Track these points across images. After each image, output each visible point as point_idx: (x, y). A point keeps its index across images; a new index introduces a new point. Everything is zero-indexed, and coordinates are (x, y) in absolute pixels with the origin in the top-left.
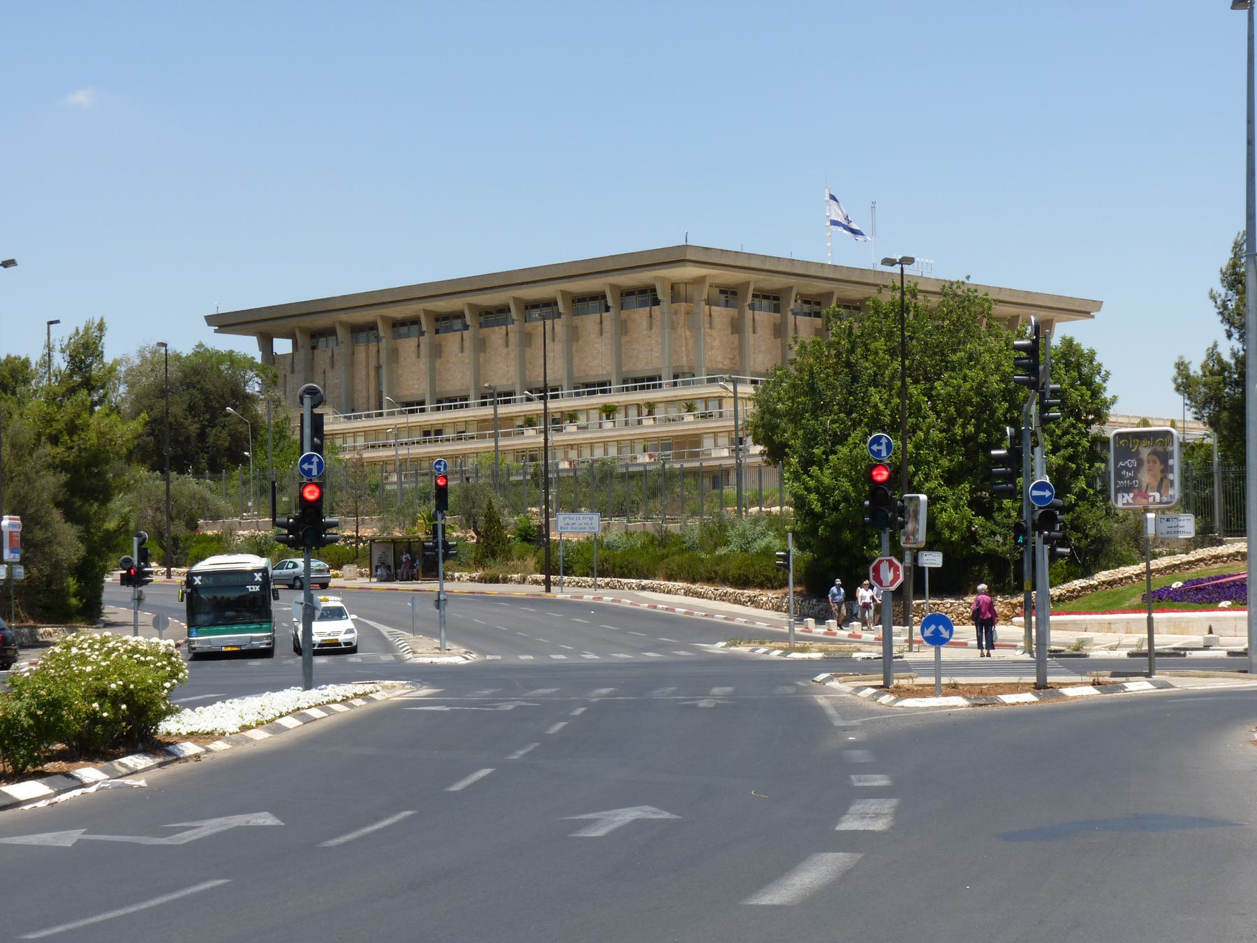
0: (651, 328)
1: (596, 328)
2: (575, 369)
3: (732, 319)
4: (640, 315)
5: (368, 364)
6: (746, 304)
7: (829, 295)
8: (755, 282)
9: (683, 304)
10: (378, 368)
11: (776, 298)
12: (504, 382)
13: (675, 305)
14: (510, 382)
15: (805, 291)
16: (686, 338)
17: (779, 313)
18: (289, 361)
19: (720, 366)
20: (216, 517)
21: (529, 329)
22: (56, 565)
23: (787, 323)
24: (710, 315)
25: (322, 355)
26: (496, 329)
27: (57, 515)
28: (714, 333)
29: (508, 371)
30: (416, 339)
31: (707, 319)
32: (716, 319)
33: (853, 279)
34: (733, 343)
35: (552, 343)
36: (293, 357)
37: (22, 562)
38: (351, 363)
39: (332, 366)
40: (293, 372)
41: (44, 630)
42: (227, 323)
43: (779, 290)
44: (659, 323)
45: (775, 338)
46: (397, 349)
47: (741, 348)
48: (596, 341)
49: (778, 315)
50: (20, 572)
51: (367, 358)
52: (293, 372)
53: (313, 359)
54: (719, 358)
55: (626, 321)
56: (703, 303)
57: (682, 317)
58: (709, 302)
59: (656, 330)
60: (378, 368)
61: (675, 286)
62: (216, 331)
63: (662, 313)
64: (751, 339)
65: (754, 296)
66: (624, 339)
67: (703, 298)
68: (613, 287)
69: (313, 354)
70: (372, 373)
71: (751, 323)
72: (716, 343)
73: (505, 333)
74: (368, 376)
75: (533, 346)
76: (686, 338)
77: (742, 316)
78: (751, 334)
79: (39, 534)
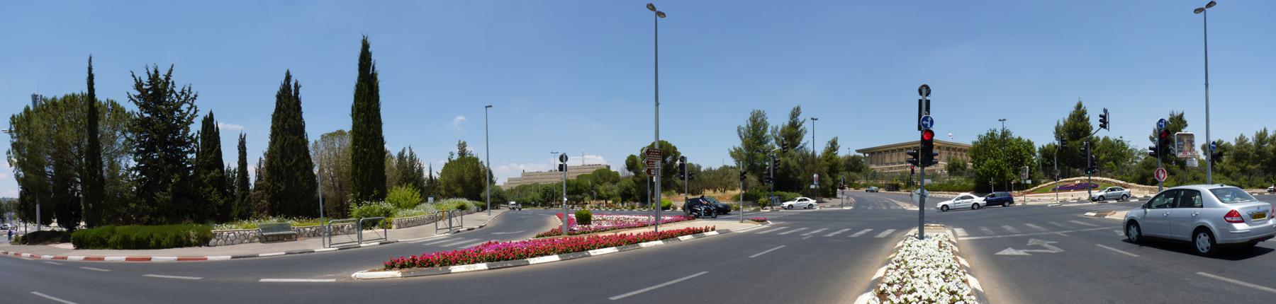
20: (857, 180)
22: (827, 186)
27: (827, 176)
37: (819, 185)
41: (824, 199)
50: (818, 187)
79: (823, 179)
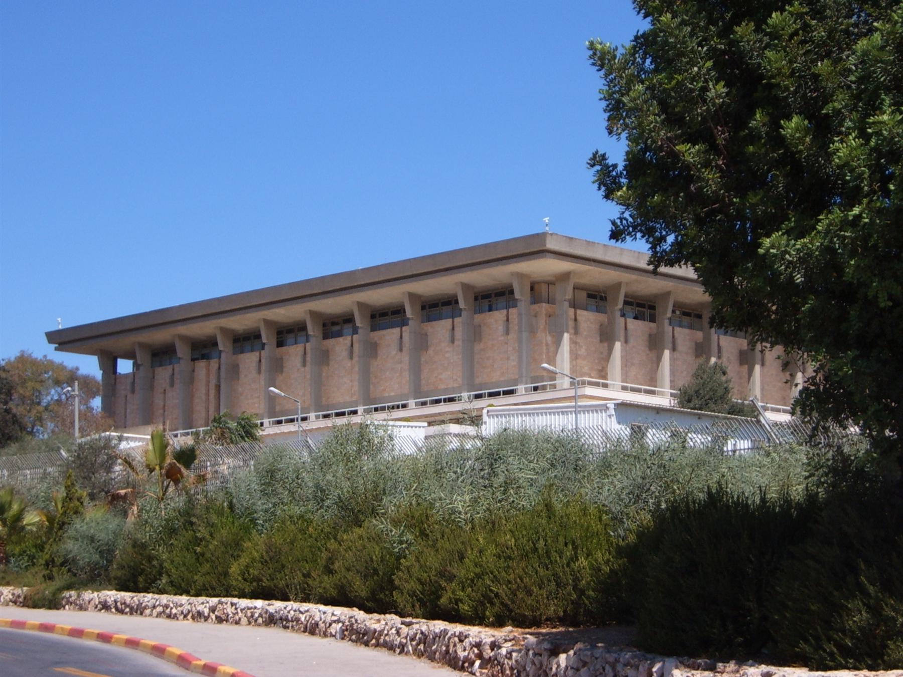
0: (507, 332)
1: (447, 335)
2: (423, 382)
4: (495, 319)
5: (208, 383)
10: (218, 387)
13: (536, 306)
16: (547, 345)
18: (130, 380)
21: (376, 339)
25: (163, 374)
29: (352, 386)
30: (258, 354)
35: (399, 353)
36: (134, 376)
38: (191, 380)
39: (172, 384)
40: (133, 391)
42: (67, 339)
44: (516, 328)
46: (238, 365)
48: (447, 349)
51: (208, 375)
52: (133, 391)
53: (154, 378)
55: (480, 326)
56: (566, 304)
57: (542, 321)
59: (513, 336)
60: (218, 387)
61: (536, 287)
62: (56, 349)
63: (520, 314)
66: (478, 347)
69: (154, 372)
70: (212, 392)
73: (349, 344)
74: (208, 394)
75: (379, 358)
76: (547, 345)
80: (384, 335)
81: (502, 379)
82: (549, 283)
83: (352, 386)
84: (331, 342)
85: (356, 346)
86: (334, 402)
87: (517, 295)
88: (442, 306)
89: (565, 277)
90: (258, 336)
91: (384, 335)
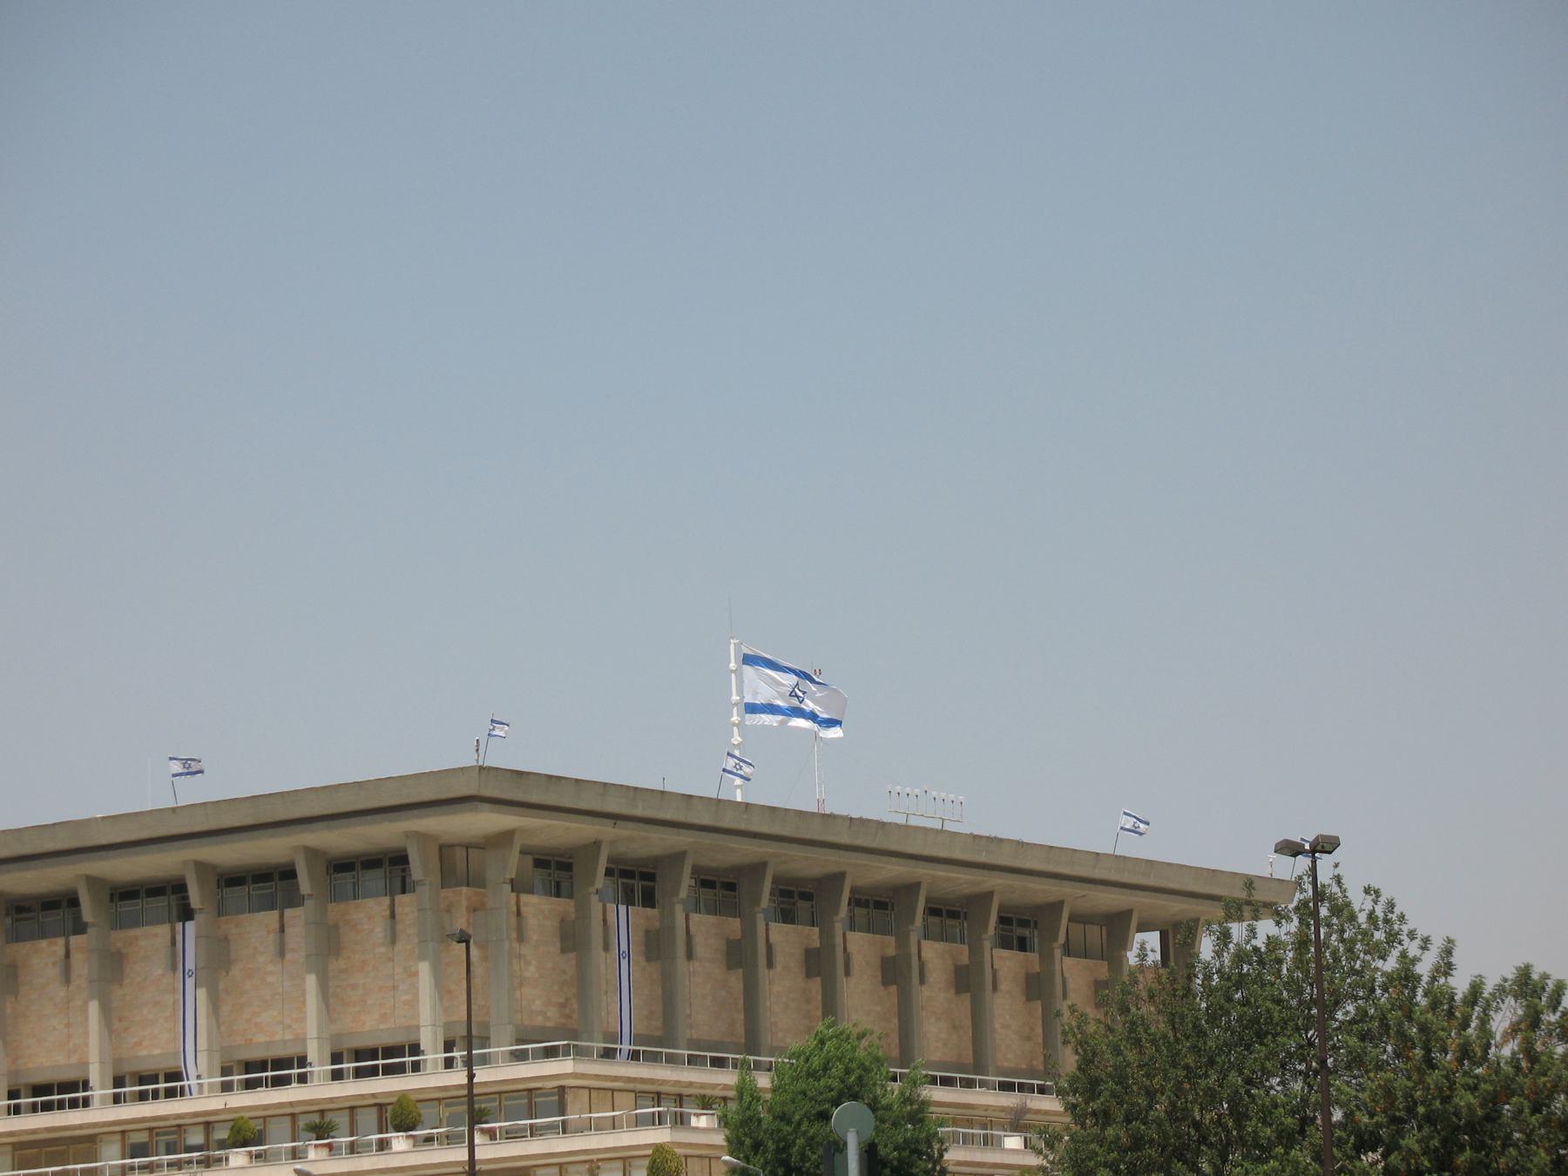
0: (393, 941)
3: (562, 921)
6: (592, 890)
7: (758, 868)
8: (612, 843)
9: (464, 889)
11: (650, 877)
12: (60, 1059)
13: (448, 893)
14: (74, 1060)
15: (707, 861)
17: (653, 906)
19: (539, 1021)
21: (119, 945)
23: (674, 928)
24: (519, 913)
26: (44, 943)
28: (527, 951)
31: (513, 919)
32: (532, 922)
33: (809, 836)
34: (564, 972)
43: (657, 860)
45: (648, 959)
47: (582, 983)
48: (270, 968)
49: (655, 911)
54: (538, 1005)
55: (336, 927)
56: (508, 887)
58: (518, 886)
64: (602, 963)
65: (609, 872)
67: (508, 877)
68: (312, 853)
71: (600, 929)
72: (531, 971)
73: (61, 952)
75: (127, 981)
77: (583, 911)
78: (603, 954)
80: (136, 938)
81: (382, 1027)
82: (467, 847)
83: (69, 1036)
84: (23, 948)
85: (77, 958)
86: (30, 1065)
87: (416, 870)
88: (148, 896)
89: (502, 839)
90: (73, 902)
91: (136, 938)
